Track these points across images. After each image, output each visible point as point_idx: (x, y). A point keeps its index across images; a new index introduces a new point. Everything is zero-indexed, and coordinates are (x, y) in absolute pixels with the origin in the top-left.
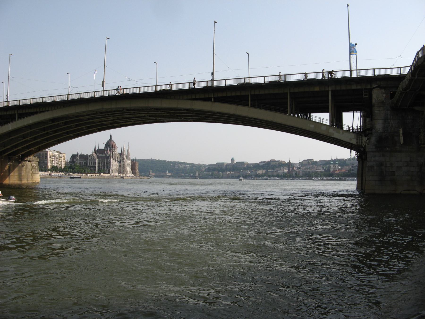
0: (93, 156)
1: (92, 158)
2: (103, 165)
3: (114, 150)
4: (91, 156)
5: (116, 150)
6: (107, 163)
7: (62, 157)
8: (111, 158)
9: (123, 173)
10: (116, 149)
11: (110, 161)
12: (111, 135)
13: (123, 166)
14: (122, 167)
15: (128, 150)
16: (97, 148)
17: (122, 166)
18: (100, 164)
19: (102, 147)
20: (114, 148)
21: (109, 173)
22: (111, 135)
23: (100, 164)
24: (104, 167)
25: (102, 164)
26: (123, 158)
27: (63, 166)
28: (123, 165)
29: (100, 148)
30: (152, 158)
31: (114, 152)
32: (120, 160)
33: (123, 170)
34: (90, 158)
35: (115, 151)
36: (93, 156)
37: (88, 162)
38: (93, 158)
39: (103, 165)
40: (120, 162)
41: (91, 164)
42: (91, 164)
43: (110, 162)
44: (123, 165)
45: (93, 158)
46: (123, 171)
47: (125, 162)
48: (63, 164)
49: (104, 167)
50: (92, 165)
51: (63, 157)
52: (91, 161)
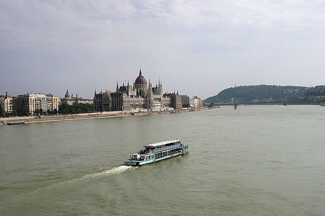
0: (106, 95)
3: (143, 86)
5: (146, 85)
6: (120, 101)
7: (52, 100)
9: (149, 108)
10: (146, 85)
12: (140, 71)
13: (149, 102)
20: (145, 84)
21: (121, 110)
22: (140, 71)
23: (114, 102)
25: (115, 101)
34: (104, 97)
36: (106, 95)
37: (103, 100)
39: (116, 102)
41: (106, 103)
43: (122, 100)
44: (149, 100)
45: (106, 96)
49: (117, 104)
52: (105, 99)
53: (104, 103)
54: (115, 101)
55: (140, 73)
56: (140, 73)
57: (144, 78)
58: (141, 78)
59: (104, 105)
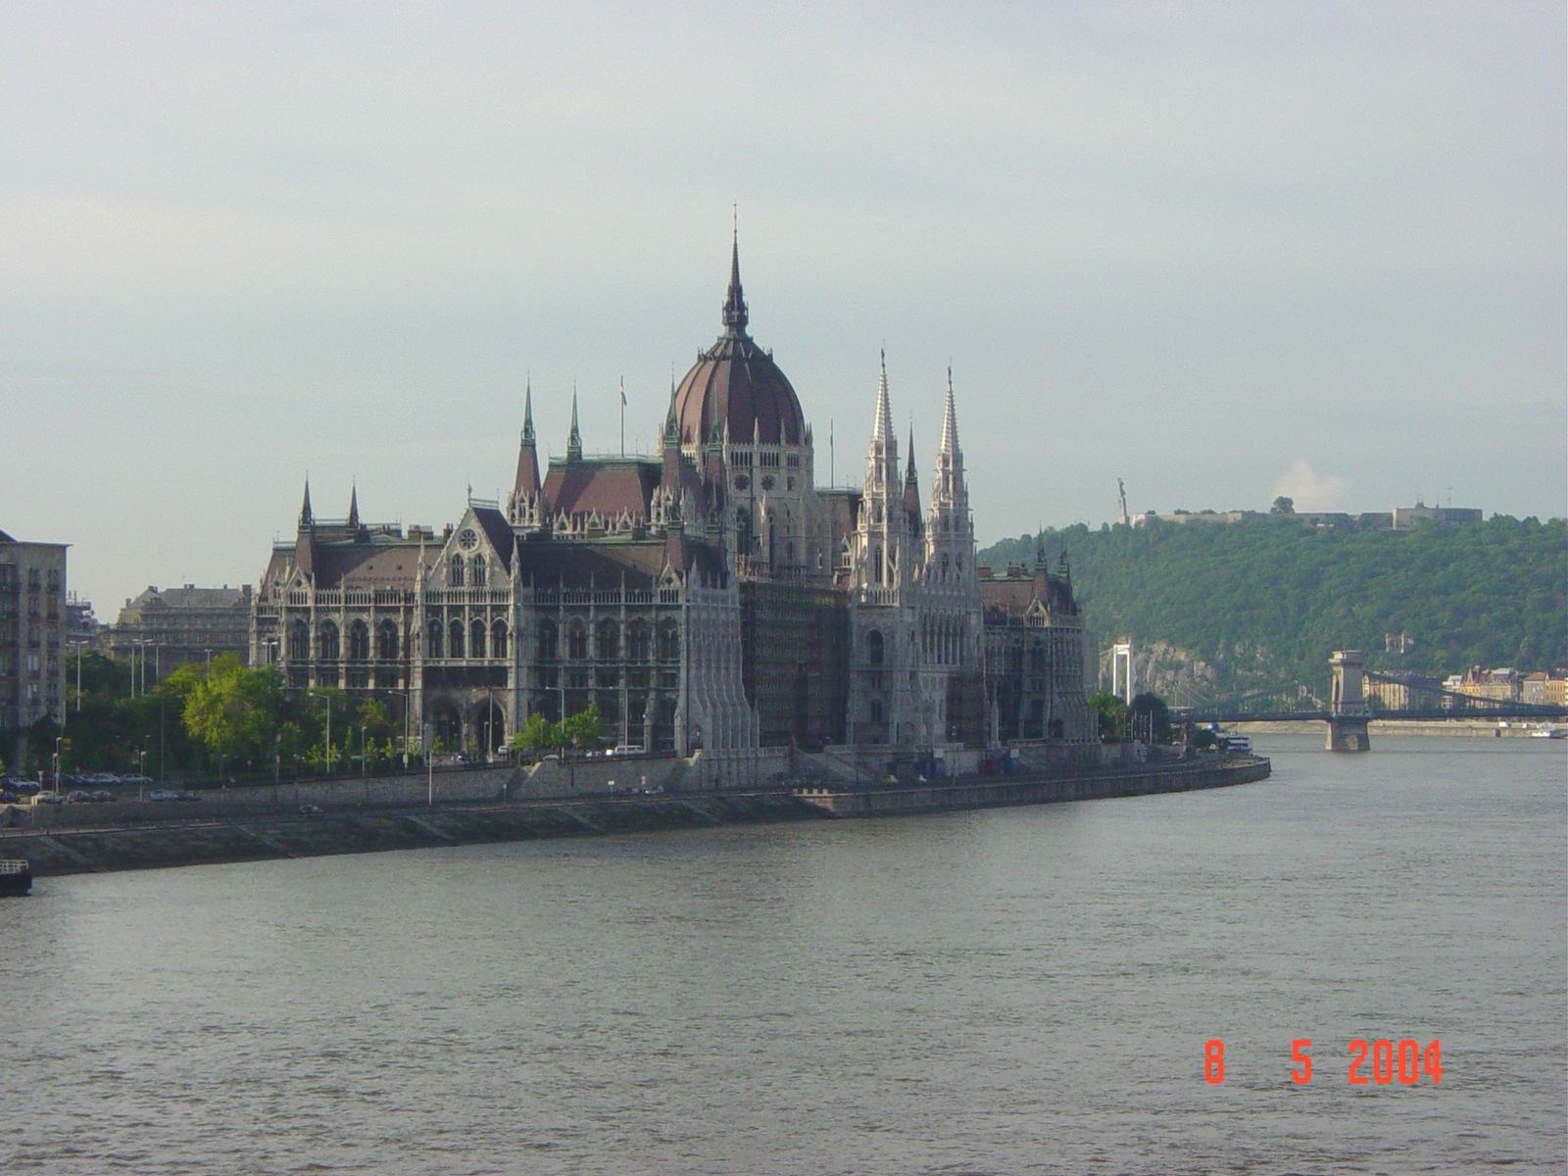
0: (466, 554)
2: (591, 649)
6: (637, 639)
12: (736, 291)
16: (552, 448)
18: (563, 649)
22: (736, 291)
23: (563, 649)
25: (578, 645)
27: (29, 693)
30: (1430, 504)
33: (877, 696)
38: (478, 577)
39: (591, 649)
48: (35, 675)
49: (607, 678)
50: (466, 661)
51: (34, 587)
52: (456, 610)
53: (435, 650)
54: (578, 645)
55: (736, 310)
56: (736, 310)
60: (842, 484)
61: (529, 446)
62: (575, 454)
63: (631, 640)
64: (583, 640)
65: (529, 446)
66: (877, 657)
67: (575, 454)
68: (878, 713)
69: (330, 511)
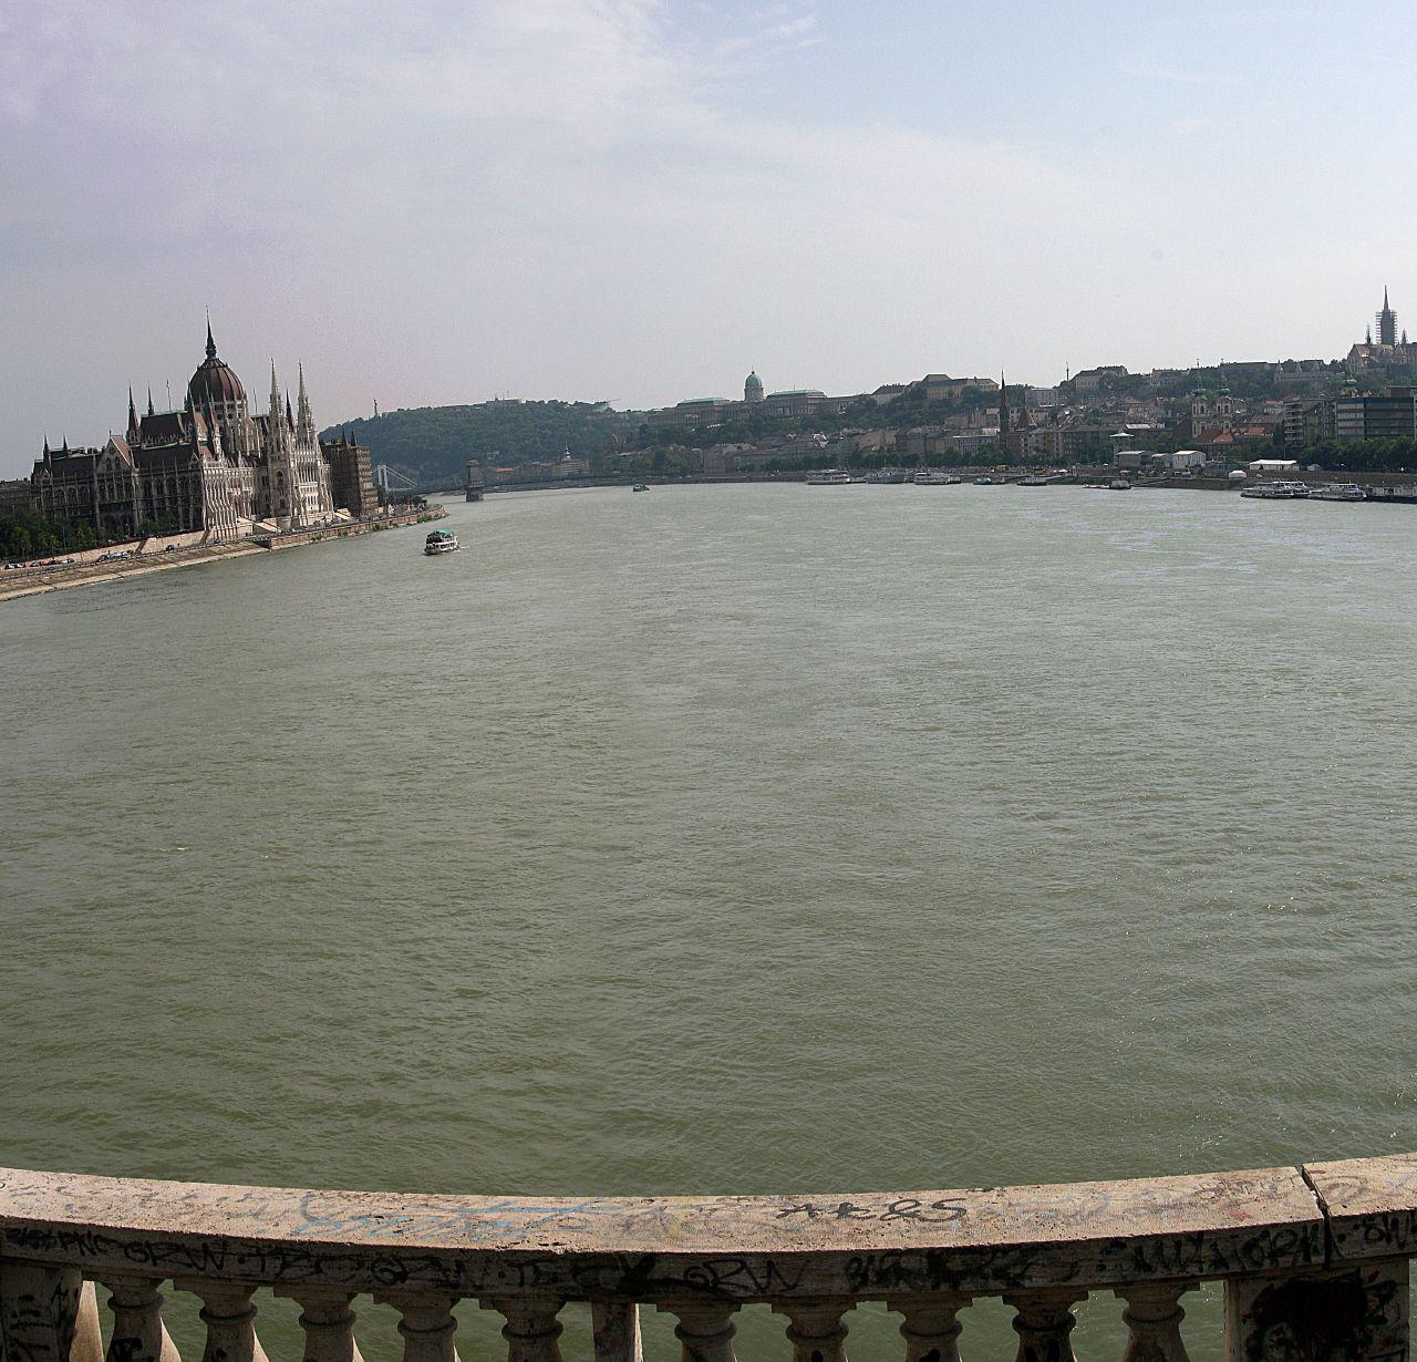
0: (112, 458)
1: (109, 467)
2: (166, 491)
3: (232, 407)
4: (106, 455)
6: (184, 485)
8: (200, 456)
11: (198, 468)
12: (210, 340)
13: (280, 482)
14: (276, 483)
15: (301, 399)
17: (274, 480)
18: (154, 492)
19: (172, 400)
21: (198, 527)
22: (210, 340)
23: (154, 492)
24: (174, 501)
25: (160, 489)
26: (274, 444)
28: (280, 474)
29: (157, 412)
31: (230, 417)
32: (264, 451)
35: (238, 410)
36: (112, 458)
37: (96, 485)
38: (118, 465)
39: (166, 491)
40: (262, 463)
41: (112, 497)
42: (112, 497)
43: (196, 477)
44: (280, 474)
45: (113, 465)
46: (283, 504)
47: (286, 461)
49: (174, 501)
54: (160, 489)
57: (229, 370)
58: (220, 370)
59: (101, 510)
60: (260, 414)
61: (132, 412)
62: (151, 411)
63: (182, 485)
64: (162, 486)
65: (132, 412)
66: (280, 482)
67: (151, 411)
68: (283, 502)
69: (56, 446)
